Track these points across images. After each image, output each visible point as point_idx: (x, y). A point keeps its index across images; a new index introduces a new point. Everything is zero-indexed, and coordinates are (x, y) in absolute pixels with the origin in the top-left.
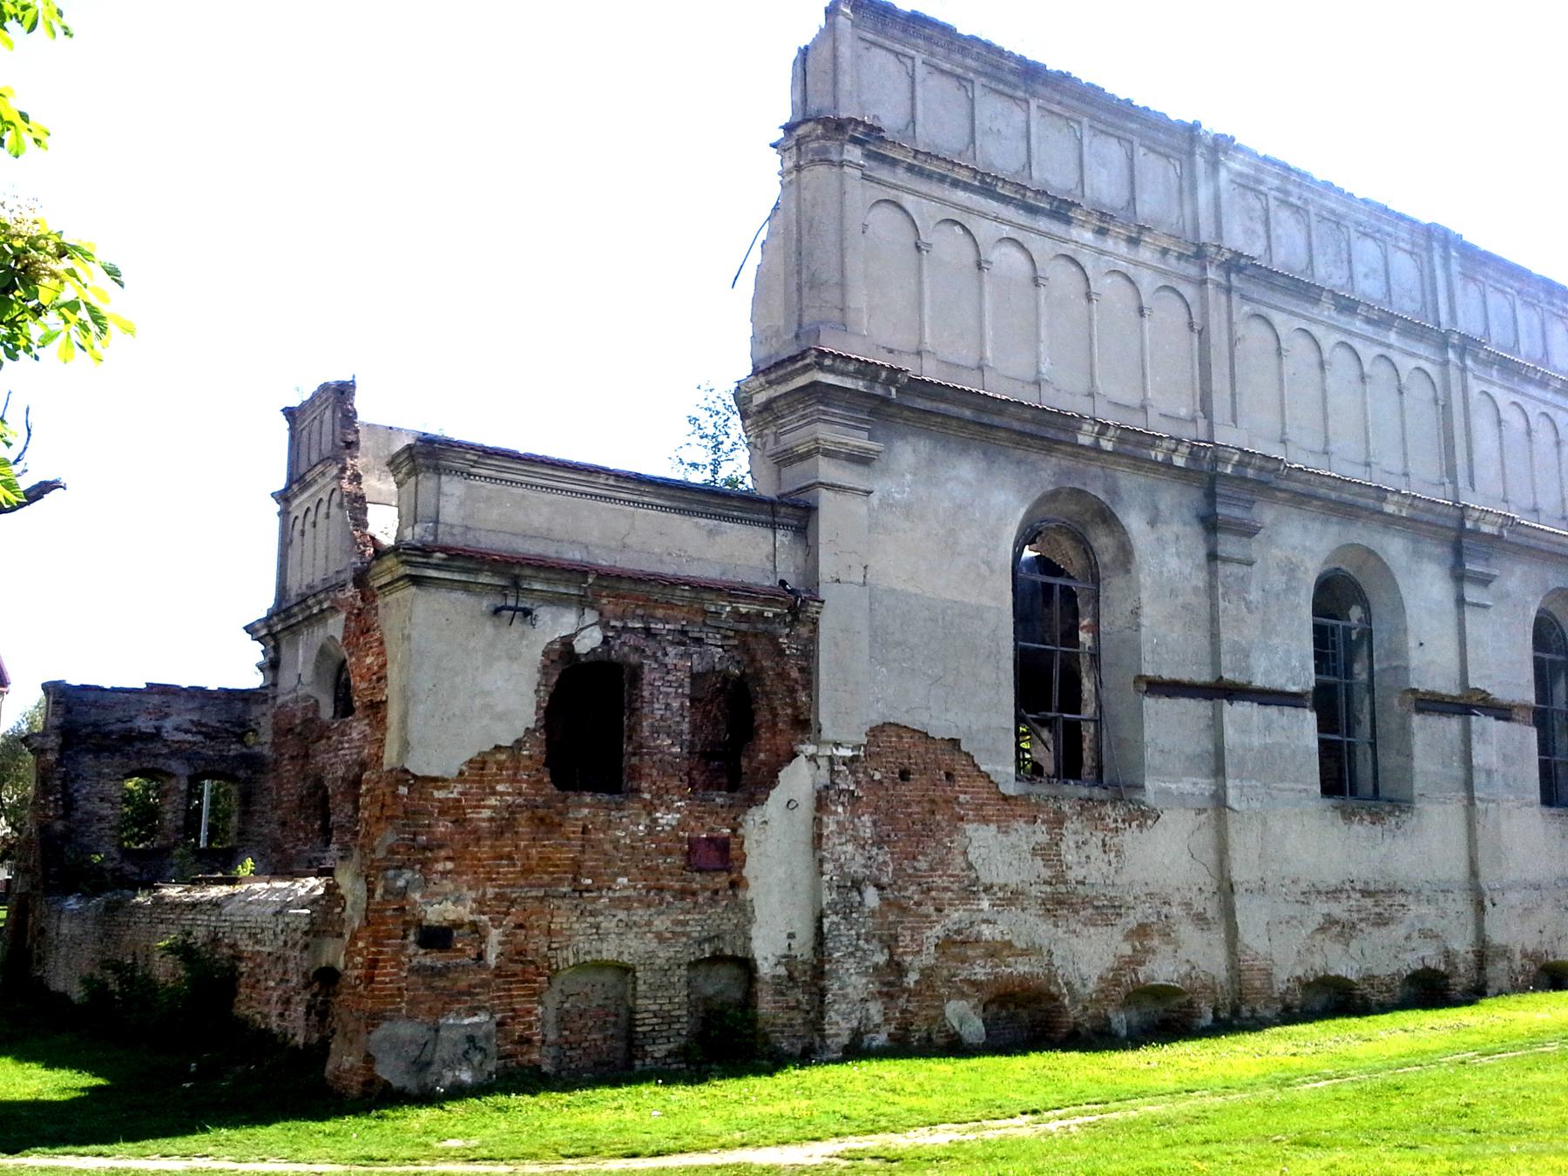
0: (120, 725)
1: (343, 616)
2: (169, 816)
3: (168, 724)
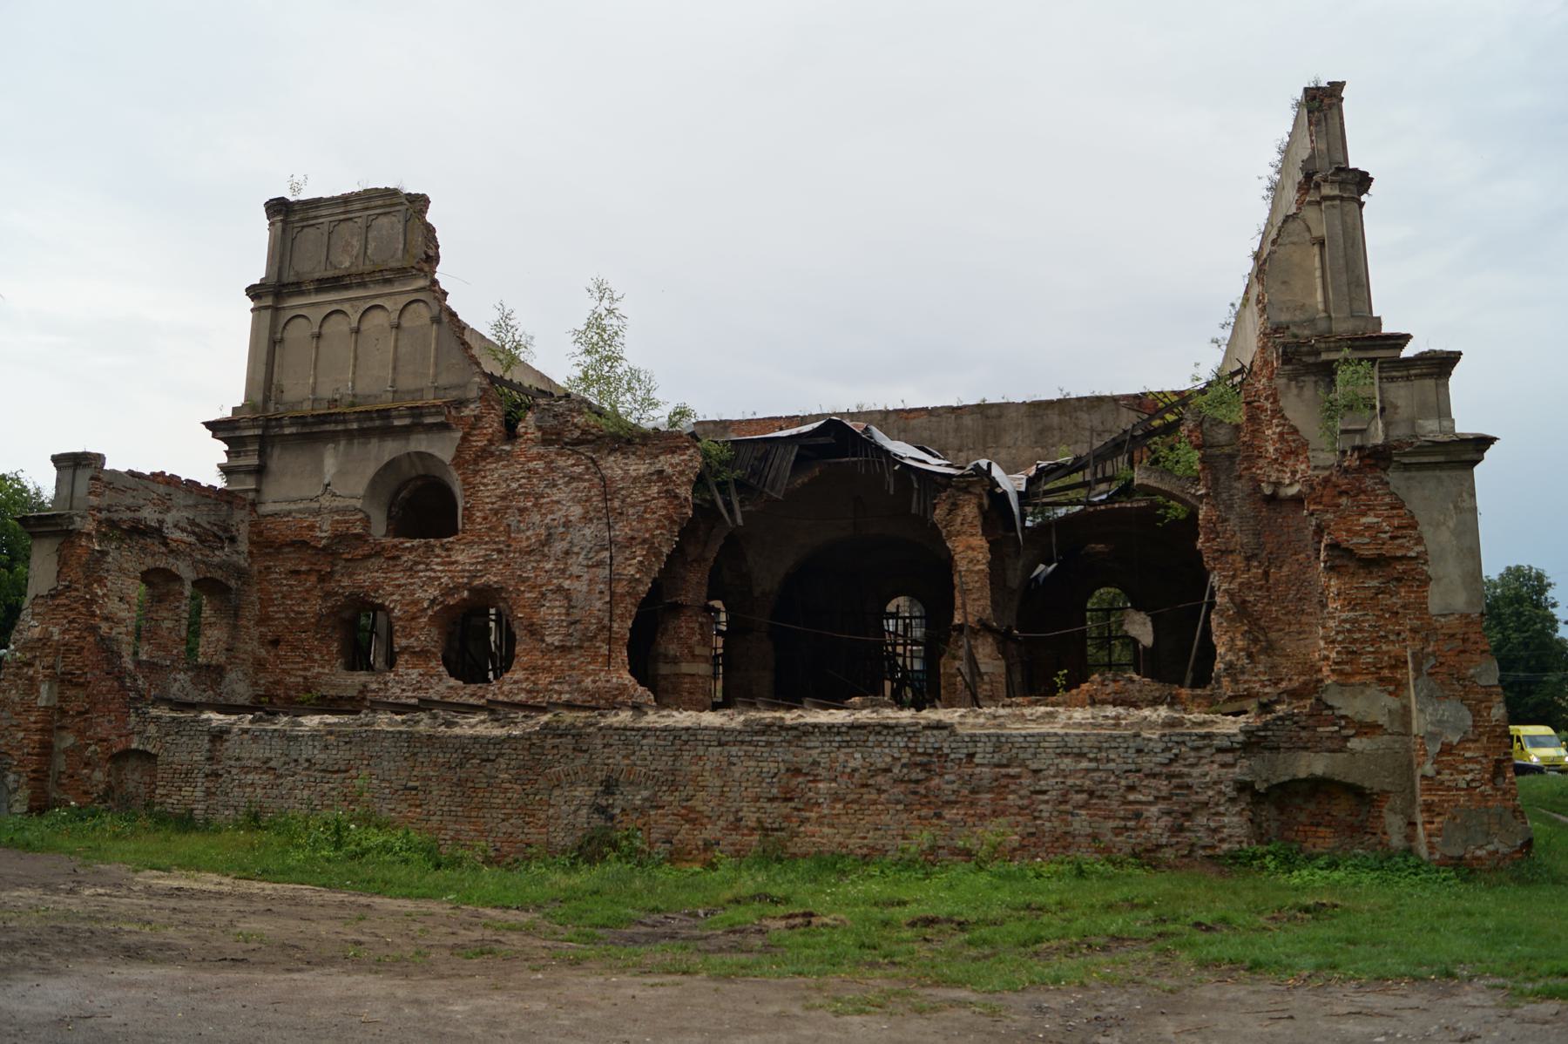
0: (130, 515)
1: (459, 435)
2: (168, 624)
3: (170, 518)
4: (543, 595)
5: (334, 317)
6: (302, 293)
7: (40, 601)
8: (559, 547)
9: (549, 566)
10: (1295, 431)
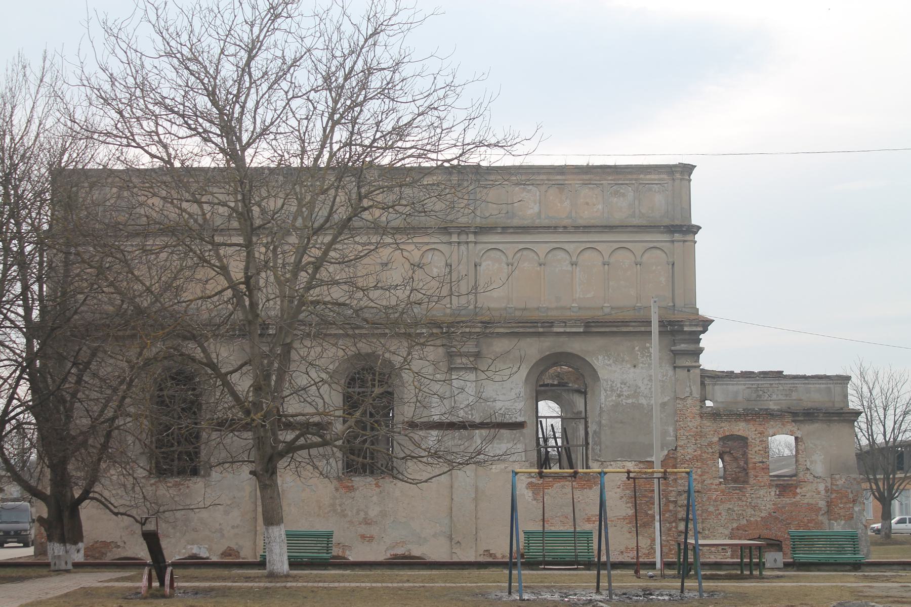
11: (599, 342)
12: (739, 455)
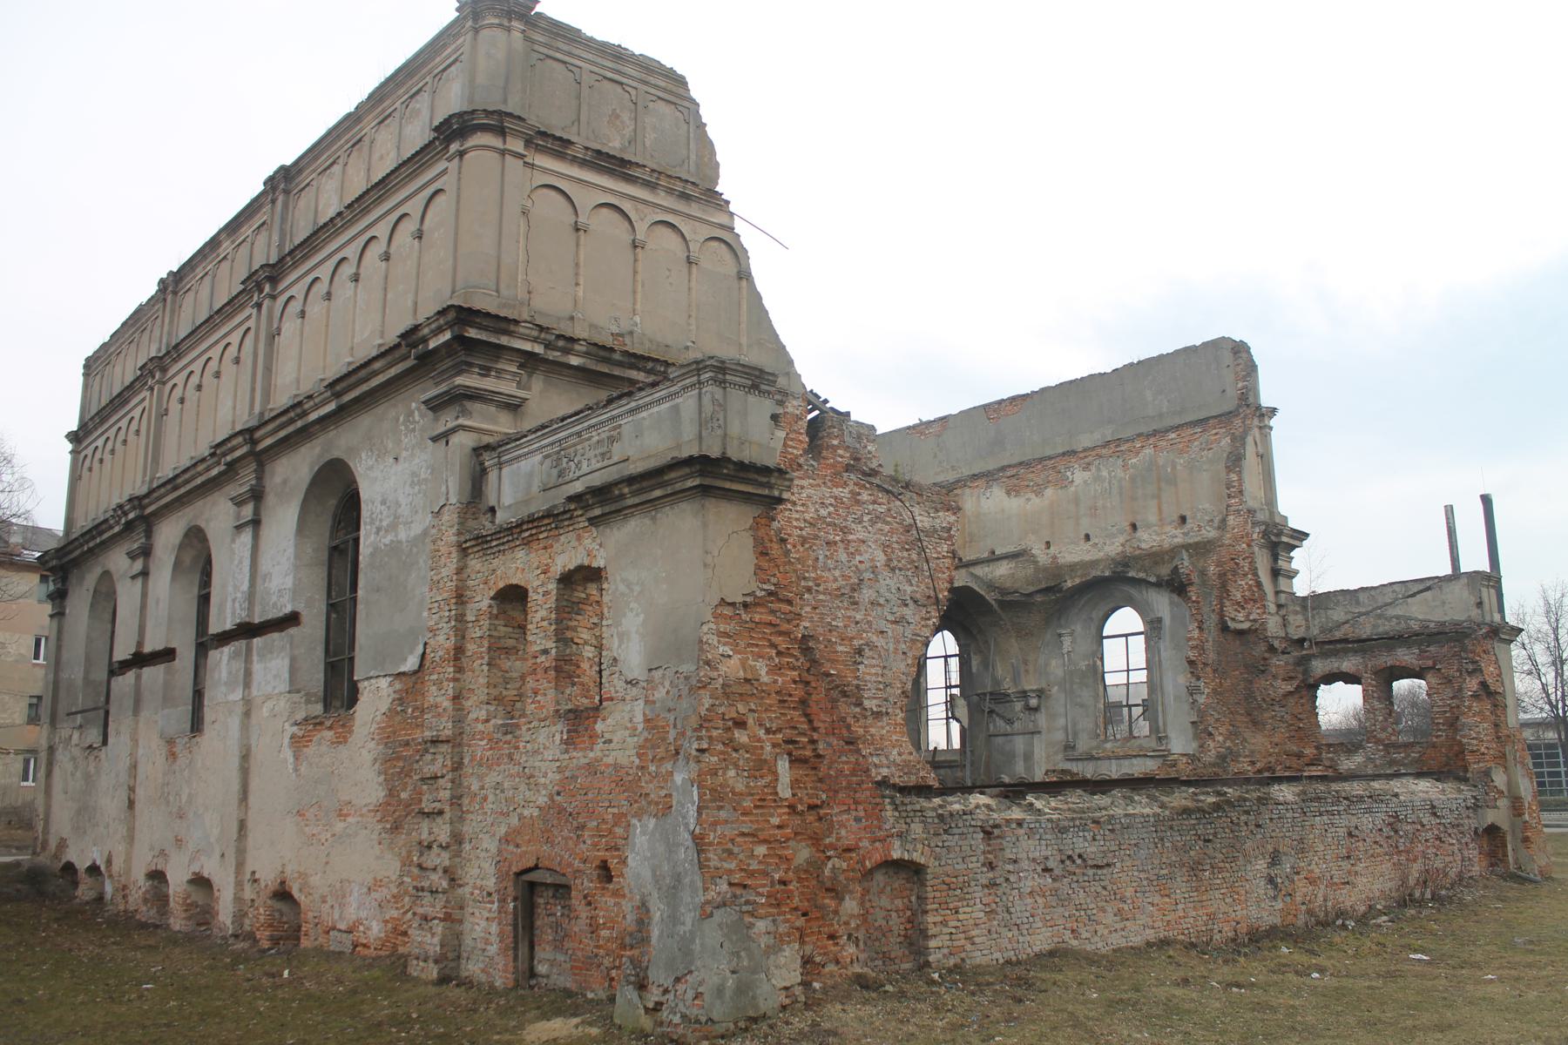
4: (860, 652)
5: (604, 210)
6: (560, 156)
7: (728, 611)
8: (867, 594)
9: (859, 617)
10: (1259, 585)
11: (364, 422)
12: (1453, 672)
